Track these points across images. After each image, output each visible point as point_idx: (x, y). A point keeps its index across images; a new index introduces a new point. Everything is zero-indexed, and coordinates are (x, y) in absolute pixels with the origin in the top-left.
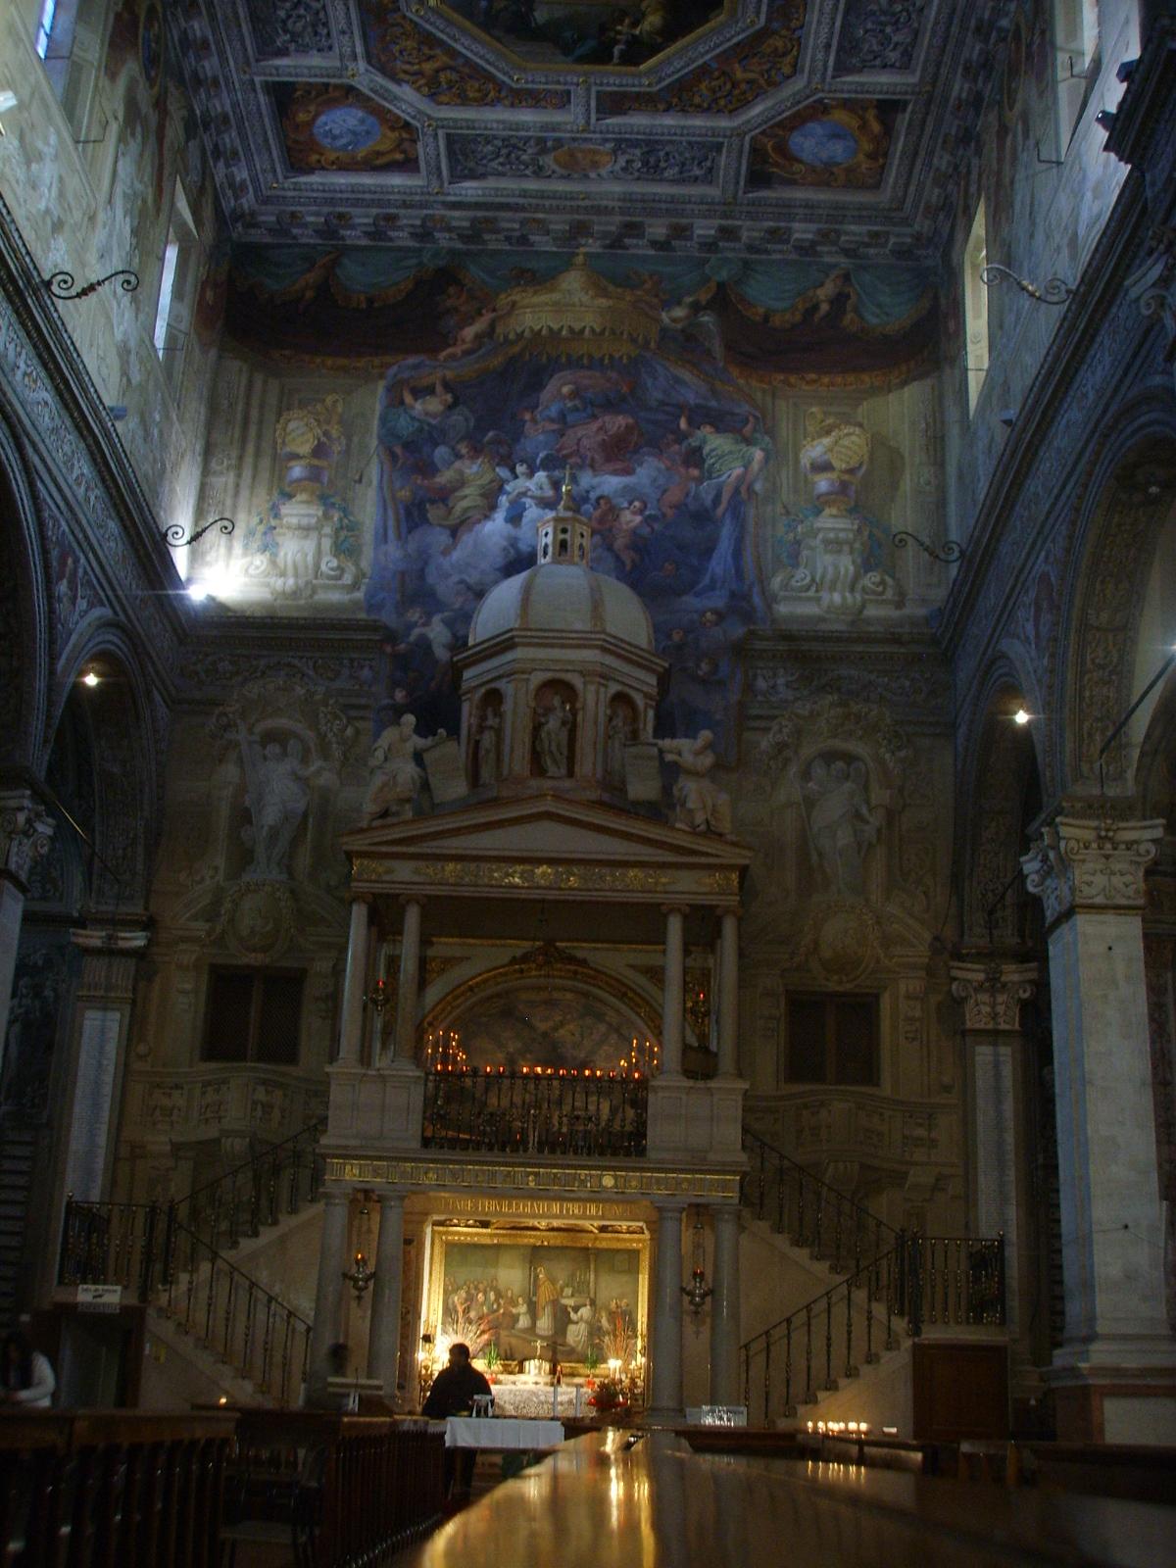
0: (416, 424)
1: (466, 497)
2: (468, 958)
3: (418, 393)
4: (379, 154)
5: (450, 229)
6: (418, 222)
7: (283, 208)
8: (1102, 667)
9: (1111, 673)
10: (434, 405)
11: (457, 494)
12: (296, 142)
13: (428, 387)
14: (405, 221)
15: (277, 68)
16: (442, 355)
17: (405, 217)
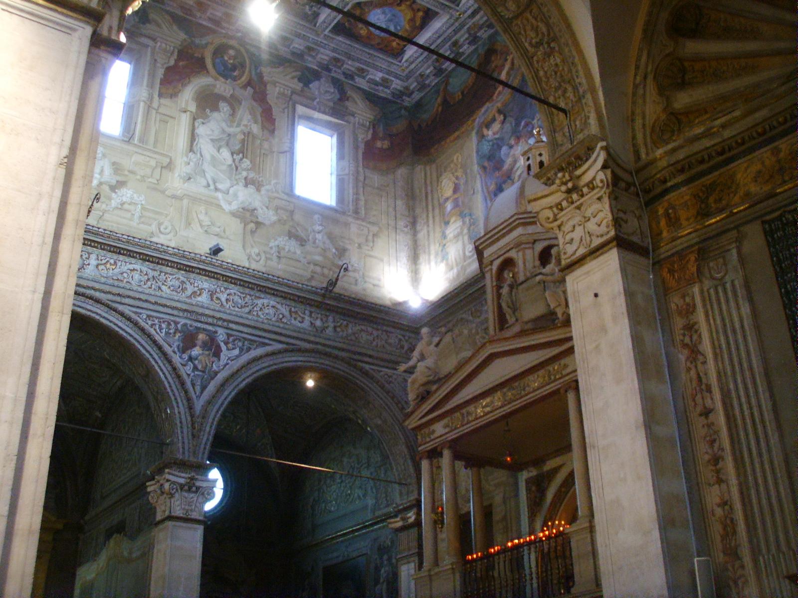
0: (491, 143)
1: (518, 169)
2: (563, 464)
3: (488, 125)
4: (412, 20)
5: (481, 28)
6: (466, 36)
7: (415, 75)
8: (539, 44)
9: (549, 44)
10: (496, 126)
11: (515, 168)
12: (378, 44)
13: (492, 119)
14: (462, 40)
15: (324, 22)
16: (494, 97)
17: (461, 37)
